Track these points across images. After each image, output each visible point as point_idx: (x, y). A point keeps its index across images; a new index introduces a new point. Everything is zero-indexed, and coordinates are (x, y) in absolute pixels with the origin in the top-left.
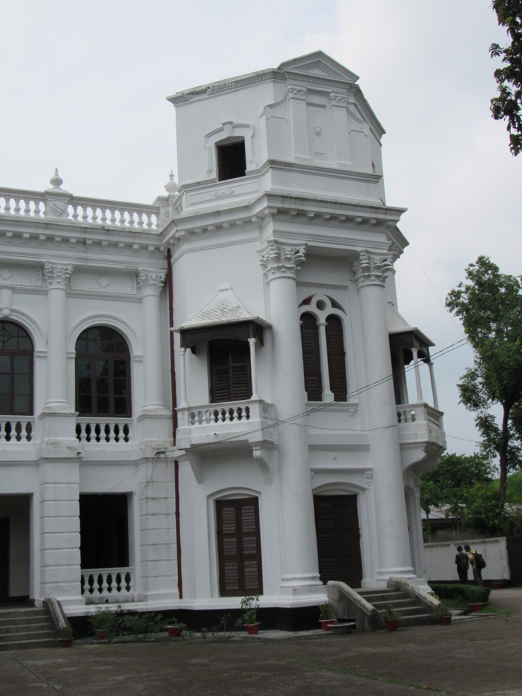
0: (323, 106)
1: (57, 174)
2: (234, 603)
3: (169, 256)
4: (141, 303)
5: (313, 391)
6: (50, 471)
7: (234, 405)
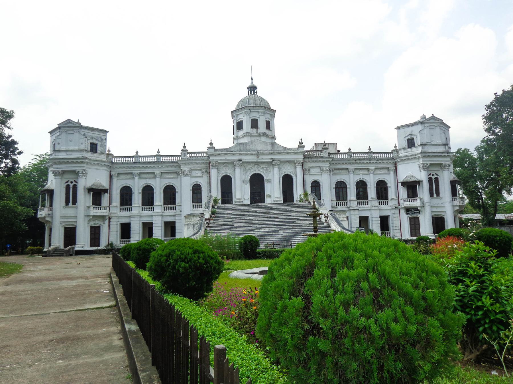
2: (415, 238)
3: (396, 164)
5: (431, 194)
6: (373, 212)
7: (414, 199)
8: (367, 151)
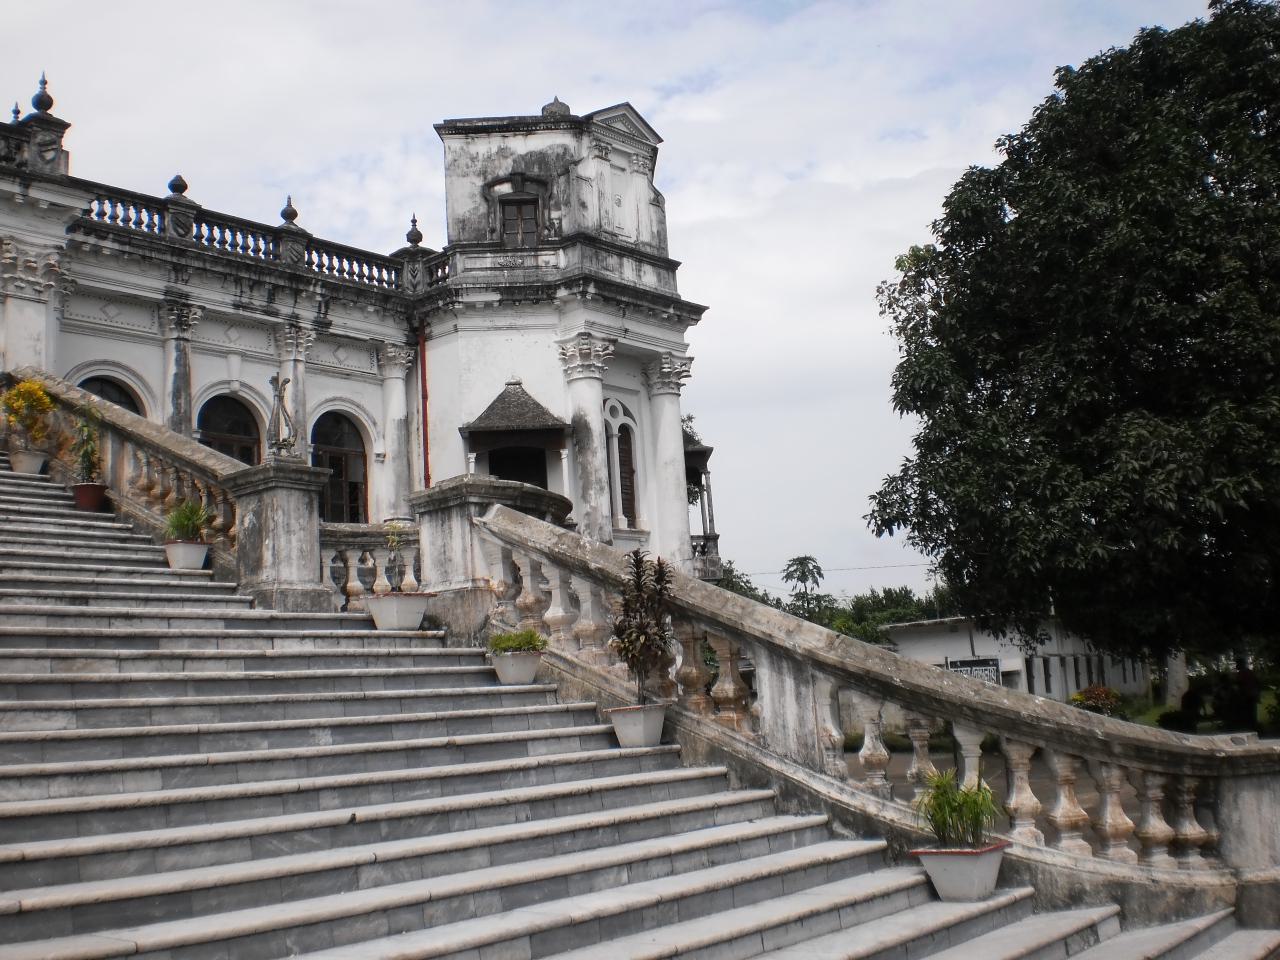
0: (623, 170)
1: (289, 205)
4: (381, 385)
8: (278, 222)
